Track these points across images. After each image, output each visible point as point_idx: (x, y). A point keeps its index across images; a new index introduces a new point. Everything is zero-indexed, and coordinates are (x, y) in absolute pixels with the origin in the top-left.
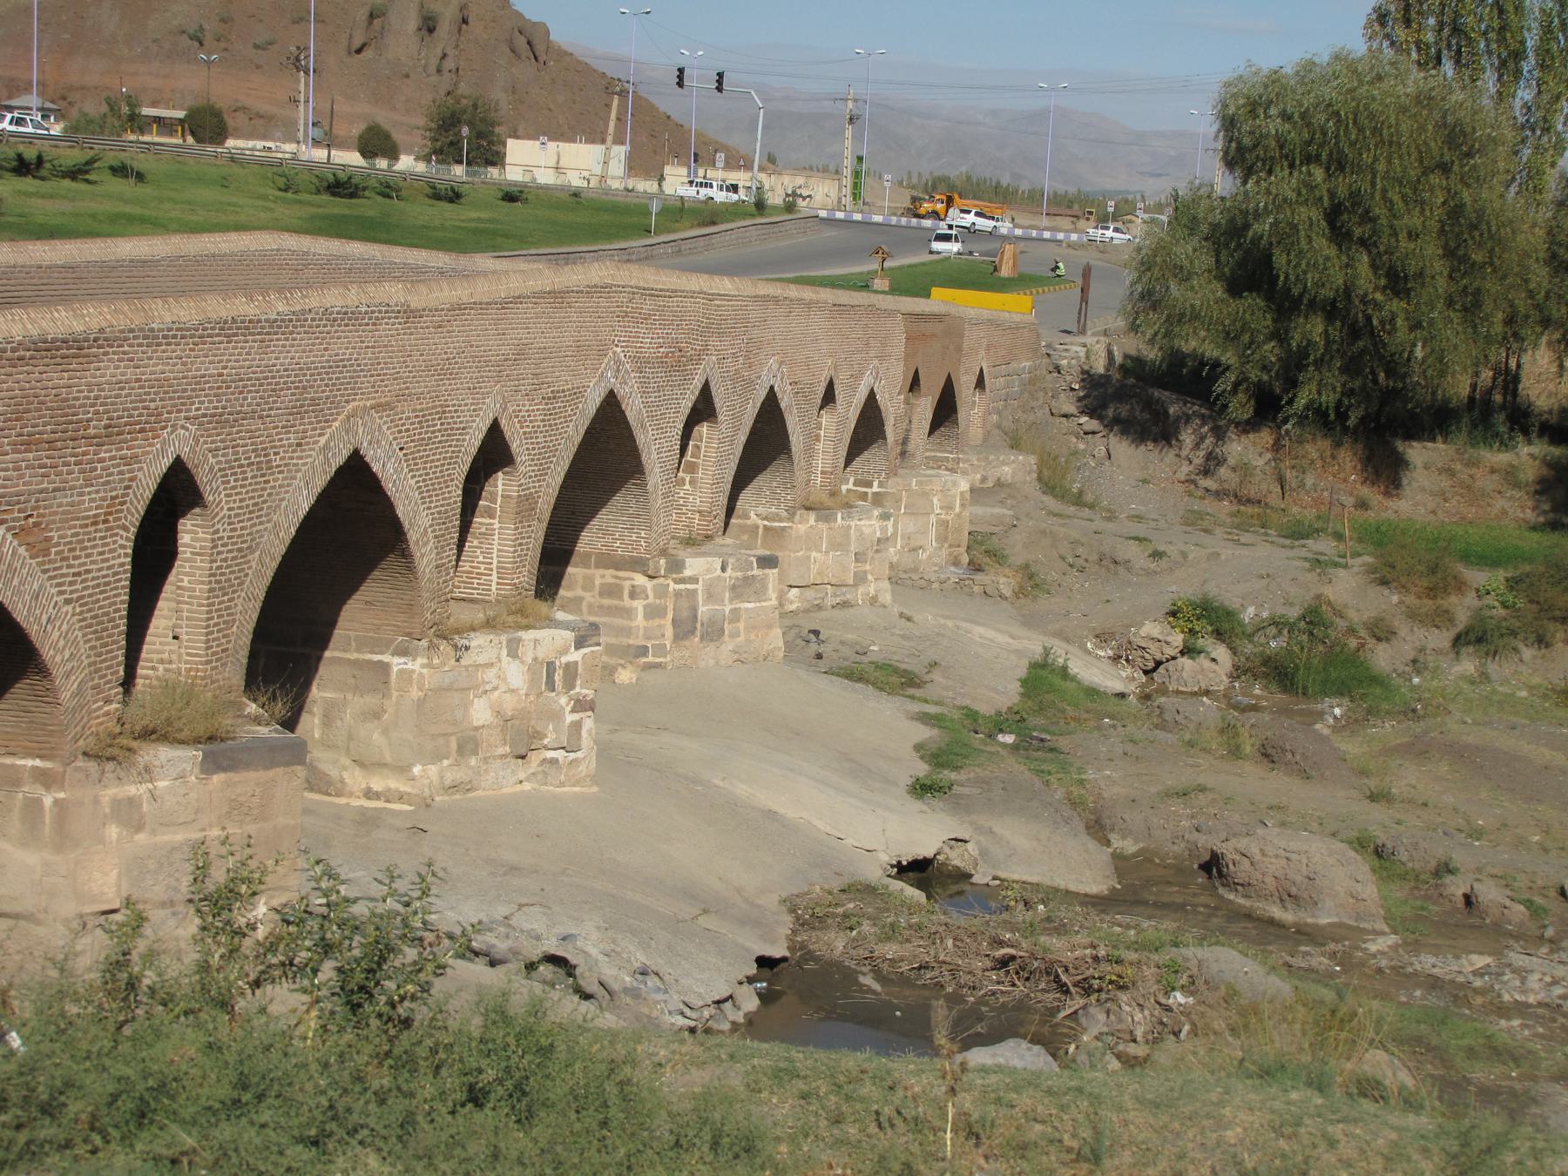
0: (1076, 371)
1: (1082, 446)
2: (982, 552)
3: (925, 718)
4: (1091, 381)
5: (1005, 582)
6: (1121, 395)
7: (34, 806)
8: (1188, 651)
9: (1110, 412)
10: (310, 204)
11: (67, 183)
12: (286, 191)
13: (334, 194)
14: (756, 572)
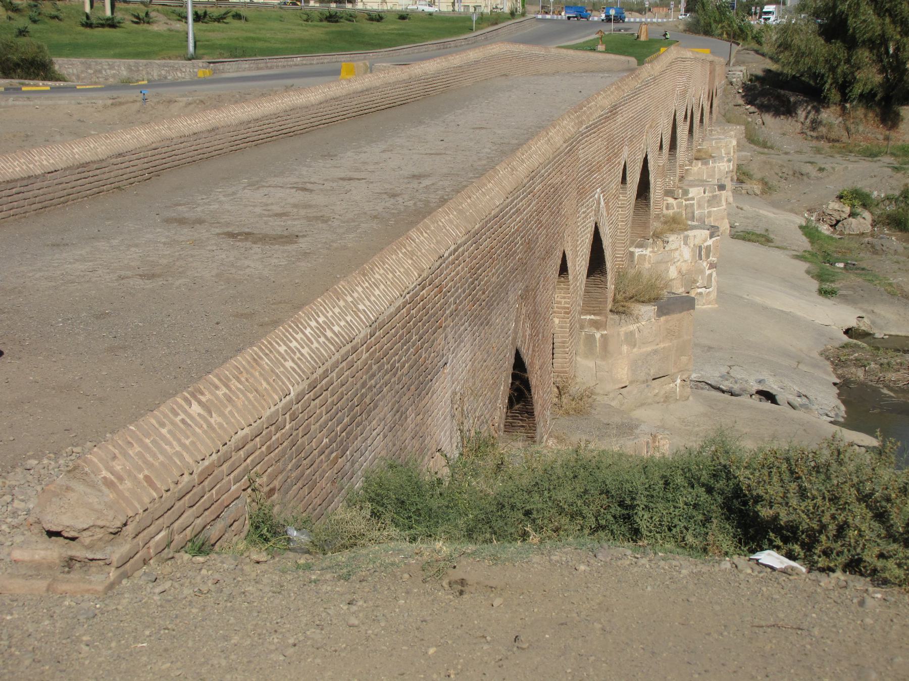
0: (740, 84)
1: (750, 120)
2: (742, 175)
3: (797, 257)
4: (746, 88)
5: (757, 188)
6: (763, 94)
7: (590, 338)
8: (852, 215)
9: (758, 102)
10: (321, 26)
11: (216, 24)
12: (307, 20)
13: (329, 21)
14: (717, 193)
